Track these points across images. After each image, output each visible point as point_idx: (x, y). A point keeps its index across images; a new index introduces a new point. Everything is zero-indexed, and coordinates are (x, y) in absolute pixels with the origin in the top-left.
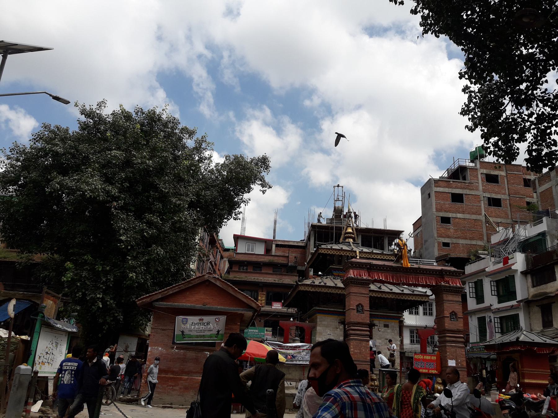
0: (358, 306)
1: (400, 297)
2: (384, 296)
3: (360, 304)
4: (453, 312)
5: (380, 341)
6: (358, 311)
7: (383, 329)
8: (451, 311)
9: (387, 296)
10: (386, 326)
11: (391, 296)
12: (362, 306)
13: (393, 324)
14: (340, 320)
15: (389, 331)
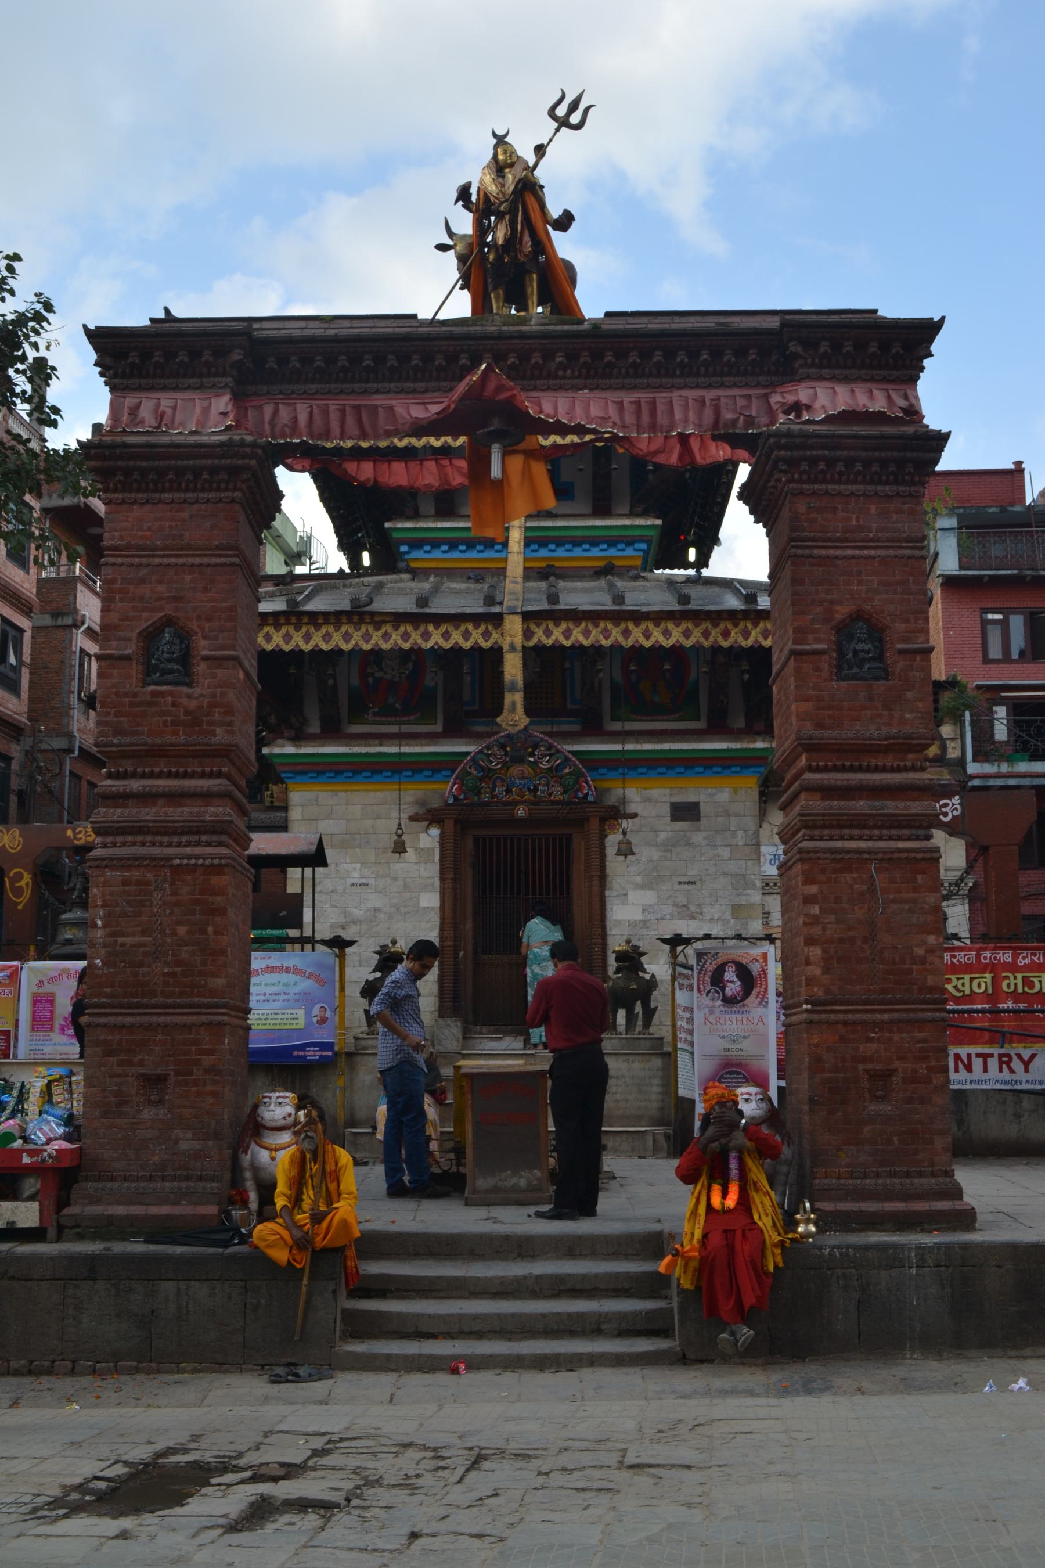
0: (150, 636)
1: (736, 638)
2: (638, 636)
3: (169, 622)
4: (857, 616)
5: (648, 897)
6: (149, 670)
7: (668, 830)
8: (842, 612)
9: (657, 637)
10: (685, 812)
11: (673, 636)
12: (184, 637)
13: (724, 796)
14: (421, 803)
15: (698, 838)
